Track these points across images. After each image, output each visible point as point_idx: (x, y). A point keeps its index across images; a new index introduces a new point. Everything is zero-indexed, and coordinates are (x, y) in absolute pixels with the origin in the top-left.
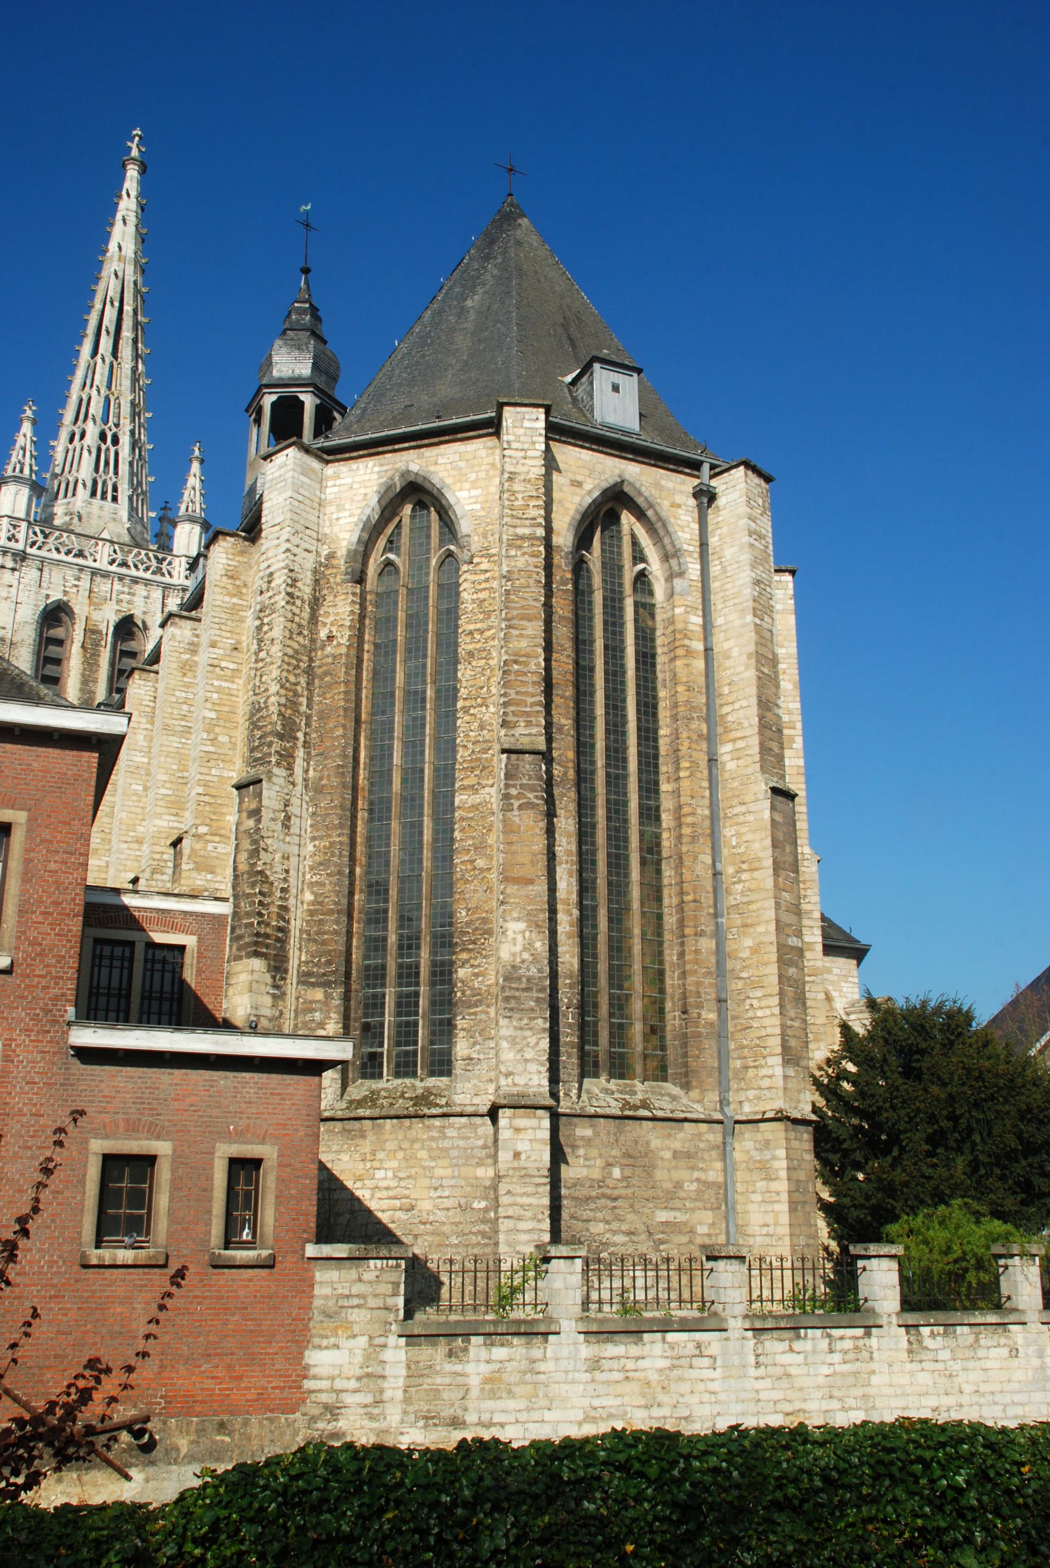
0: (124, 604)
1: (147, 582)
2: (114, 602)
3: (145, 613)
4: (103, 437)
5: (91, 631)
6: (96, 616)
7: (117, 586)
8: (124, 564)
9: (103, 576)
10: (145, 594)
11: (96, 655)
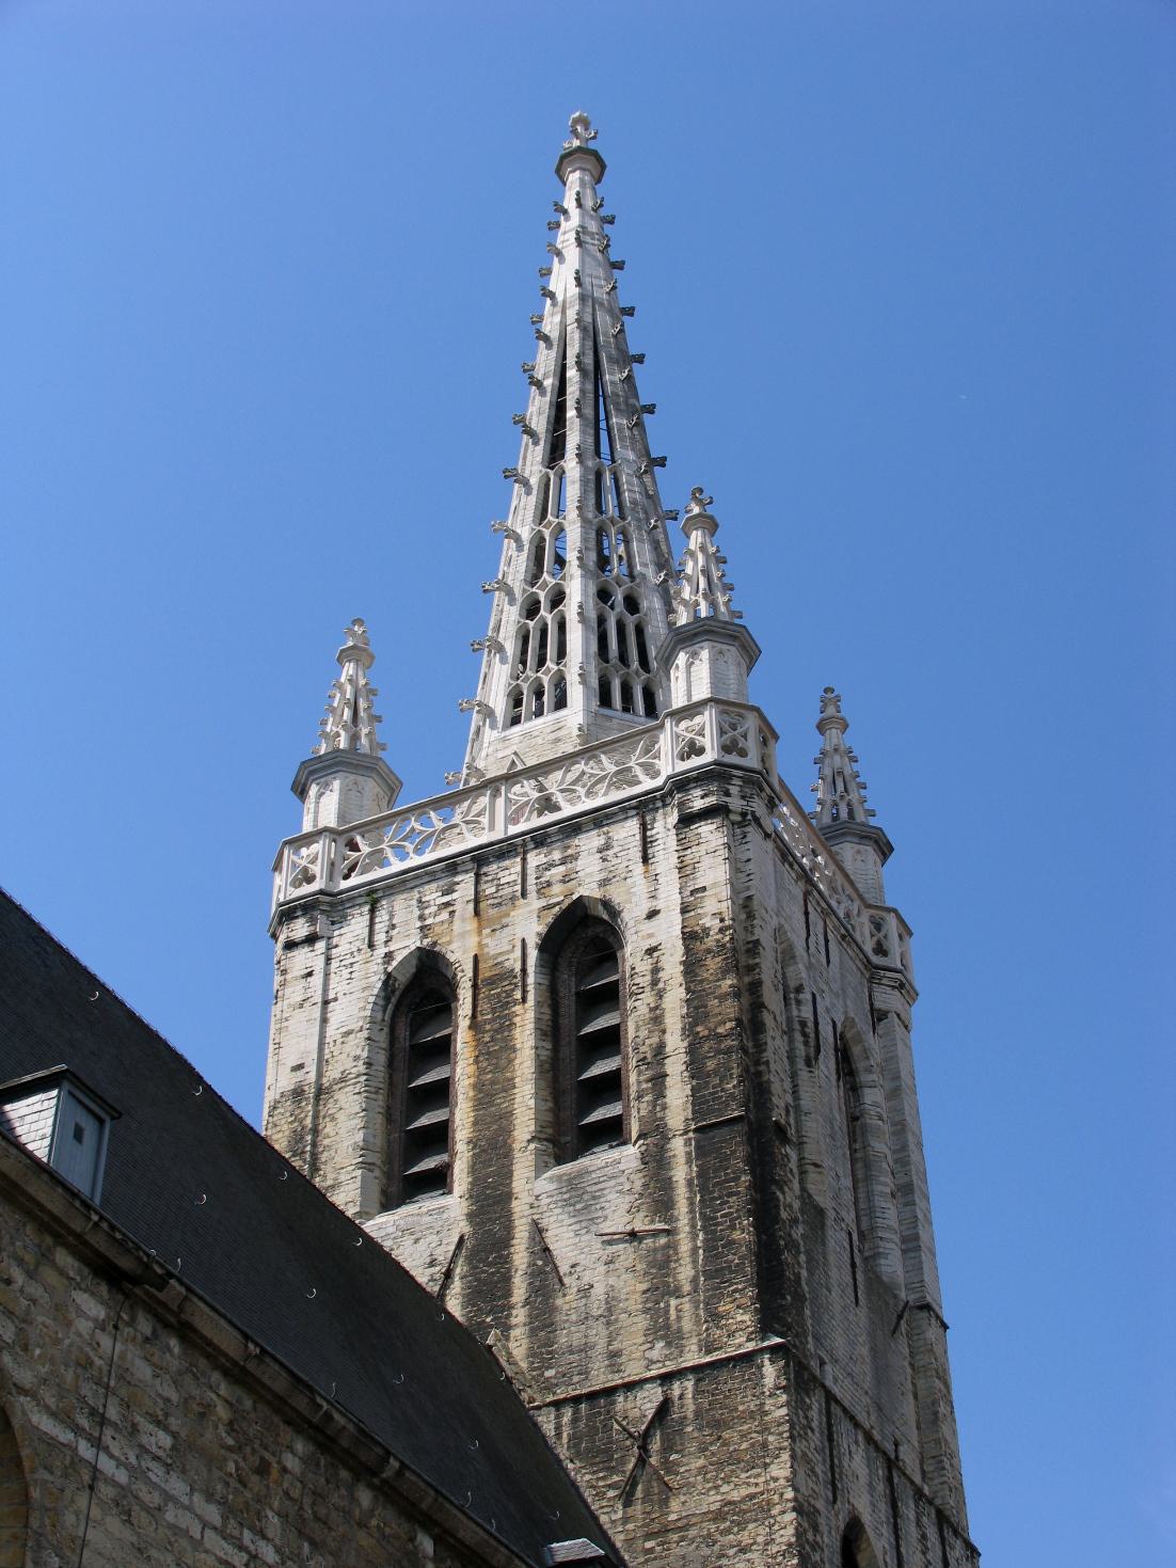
0: (557, 889)
1: (599, 818)
3: (604, 883)
5: (493, 983)
11: (506, 1026)
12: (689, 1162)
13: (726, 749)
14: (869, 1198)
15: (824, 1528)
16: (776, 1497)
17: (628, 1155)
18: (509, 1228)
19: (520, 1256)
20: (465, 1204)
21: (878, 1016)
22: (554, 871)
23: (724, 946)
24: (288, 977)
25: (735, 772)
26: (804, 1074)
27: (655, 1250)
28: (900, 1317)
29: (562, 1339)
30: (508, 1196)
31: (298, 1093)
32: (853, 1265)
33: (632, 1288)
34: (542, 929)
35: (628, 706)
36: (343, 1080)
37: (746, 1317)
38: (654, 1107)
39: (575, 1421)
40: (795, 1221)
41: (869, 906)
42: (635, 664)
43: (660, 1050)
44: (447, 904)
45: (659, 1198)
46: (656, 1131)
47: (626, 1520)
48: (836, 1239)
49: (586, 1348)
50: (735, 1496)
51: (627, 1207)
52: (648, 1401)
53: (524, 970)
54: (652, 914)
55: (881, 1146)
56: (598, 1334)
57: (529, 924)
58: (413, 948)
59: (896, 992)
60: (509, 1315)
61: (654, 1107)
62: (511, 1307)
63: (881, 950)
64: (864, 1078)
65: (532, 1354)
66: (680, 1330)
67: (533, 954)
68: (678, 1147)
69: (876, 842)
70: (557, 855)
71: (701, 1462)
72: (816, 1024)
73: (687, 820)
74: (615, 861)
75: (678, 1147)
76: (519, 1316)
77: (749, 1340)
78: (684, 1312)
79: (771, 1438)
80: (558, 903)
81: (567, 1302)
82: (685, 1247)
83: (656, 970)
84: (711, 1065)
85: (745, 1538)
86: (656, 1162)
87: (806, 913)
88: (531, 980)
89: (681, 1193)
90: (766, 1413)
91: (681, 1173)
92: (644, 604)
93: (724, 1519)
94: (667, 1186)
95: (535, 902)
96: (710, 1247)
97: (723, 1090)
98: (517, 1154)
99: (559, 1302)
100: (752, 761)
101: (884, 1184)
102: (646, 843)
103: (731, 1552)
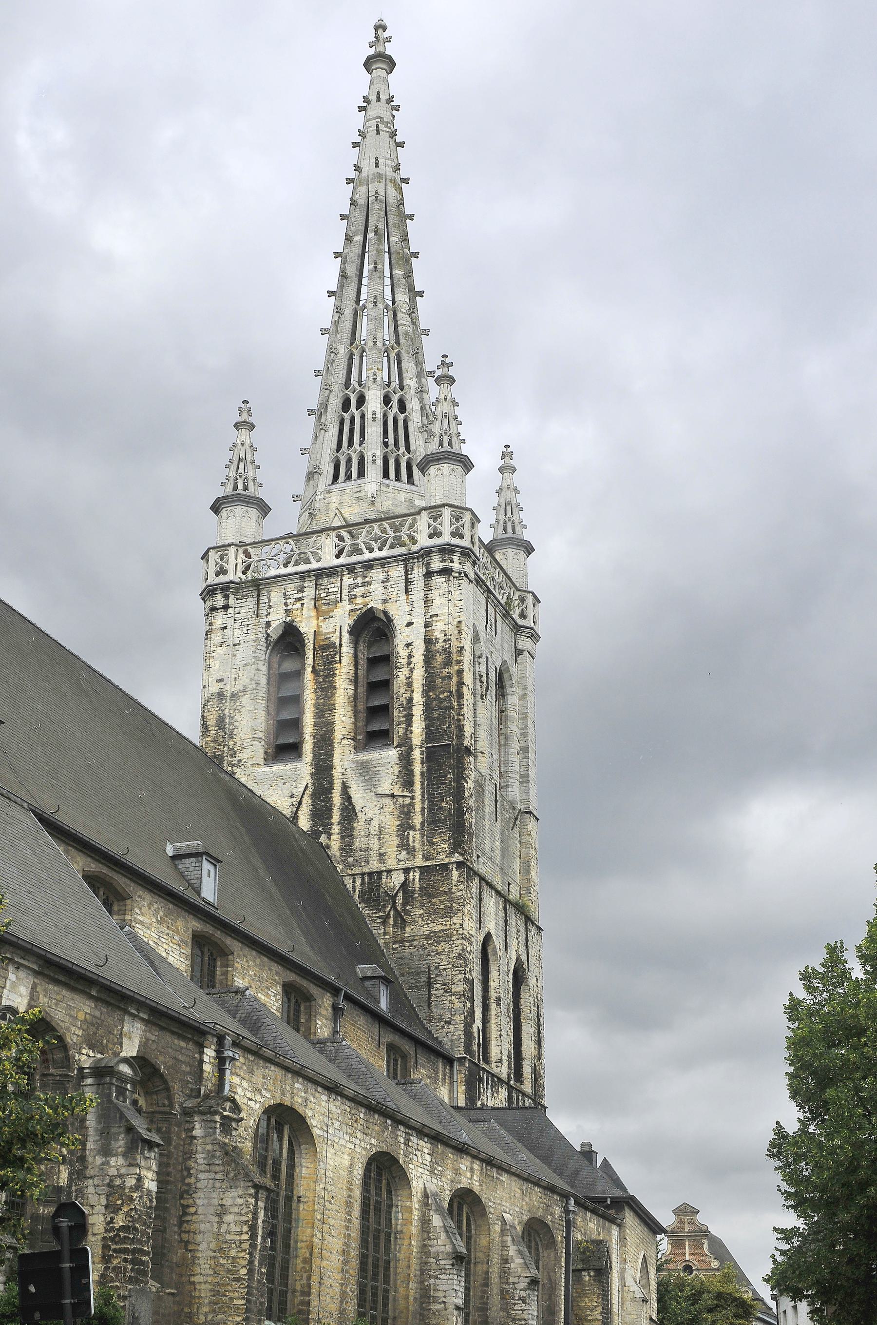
0: (359, 600)
1: (383, 562)
2: (345, 603)
3: (385, 601)
4: (387, 400)
6: (326, 627)
7: (348, 580)
8: (357, 551)
9: (330, 575)
10: (382, 576)
12: (422, 763)
13: (453, 534)
14: (507, 753)
15: (474, 944)
16: (455, 932)
17: (392, 754)
18: (331, 783)
19: (337, 799)
20: (309, 768)
21: (518, 652)
22: (358, 589)
23: (445, 649)
24: (213, 627)
25: (457, 549)
26: (480, 703)
27: (404, 806)
28: (516, 819)
29: (357, 844)
30: (331, 767)
31: (220, 695)
32: (496, 801)
33: (391, 823)
34: (351, 622)
35: (398, 478)
36: (244, 691)
37: (446, 846)
38: (406, 731)
39: (362, 884)
40: (471, 795)
41: (520, 590)
42: (402, 449)
43: (410, 700)
44: (300, 599)
45: (408, 783)
46: (406, 744)
47: (385, 934)
48: (489, 789)
49: (367, 850)
50: (436, 929)
51: (391, 782)
52: (398, 879)
53: (341, 645)
54: (410, 624)
55: (514, 727)
56: (374, 843)
57: (342, 618)
58: (281, 621)
59: (530, 640)
60: (331, 828)
61: (406, 731)
62: (332, 824)
63: (523, 615)
64: (509, 690)
65: (341, 849)
66: (414, 847)
67: (346, 637)
68: (417, 754)
69: (526, 548)
70: (360, 580)
71: (421, 912)
72: (487, 674)
73: (429, 575)
74: (391, 590)
75: (417, 754)
76: (336, 829)
77: (446, 857)
78: (415, 837)
79: (454, 905)
80: (360, 609)
81: (359, 826)
82: (418, 807)
83: (410, 656)
84: (436, 714)
85: (439, 948)
86: (406, 760)
87: (487, 611)
88: (344, 649)
89: (417, 779)
90: (453, 893)
91: (417, 768)
92: (408, 406)
93: (431, 939)
94: (411, 773)
95: (345, 607)
96: (431, 810)
97: (441, 729)
98: (336, 745)
99: (355, 825)
100: (465, 543)
101: (515, 746)
102: (408, 582)
103: (433, 954)
